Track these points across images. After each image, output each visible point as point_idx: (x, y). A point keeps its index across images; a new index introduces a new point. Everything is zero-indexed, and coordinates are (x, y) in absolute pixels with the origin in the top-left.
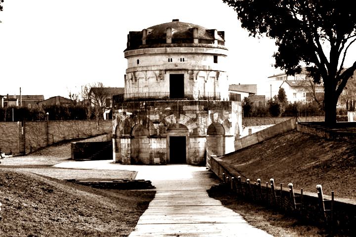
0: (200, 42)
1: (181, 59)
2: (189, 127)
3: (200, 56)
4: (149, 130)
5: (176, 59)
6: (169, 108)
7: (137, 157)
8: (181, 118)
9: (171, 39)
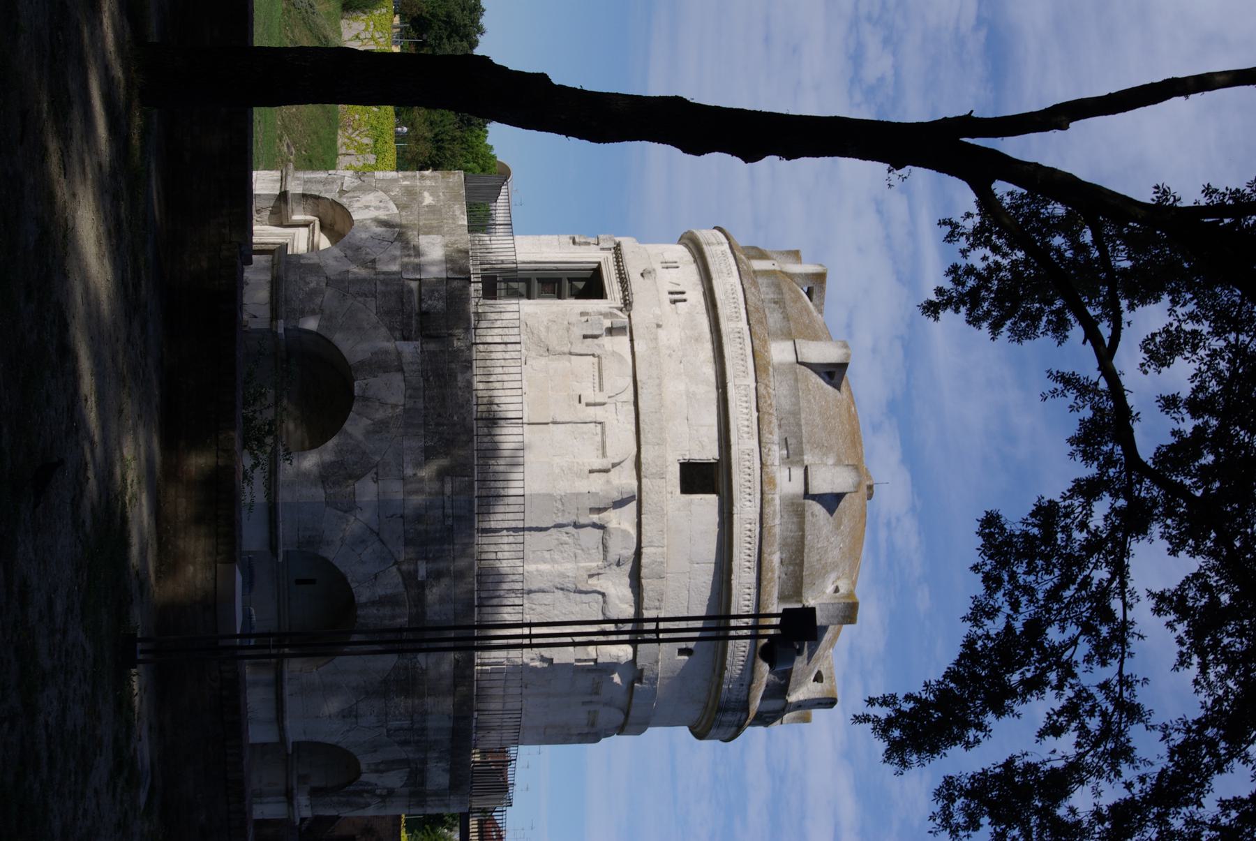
0: (782, 369)
1: (683, 293)
3: (709, 372)
6: (428, 199)
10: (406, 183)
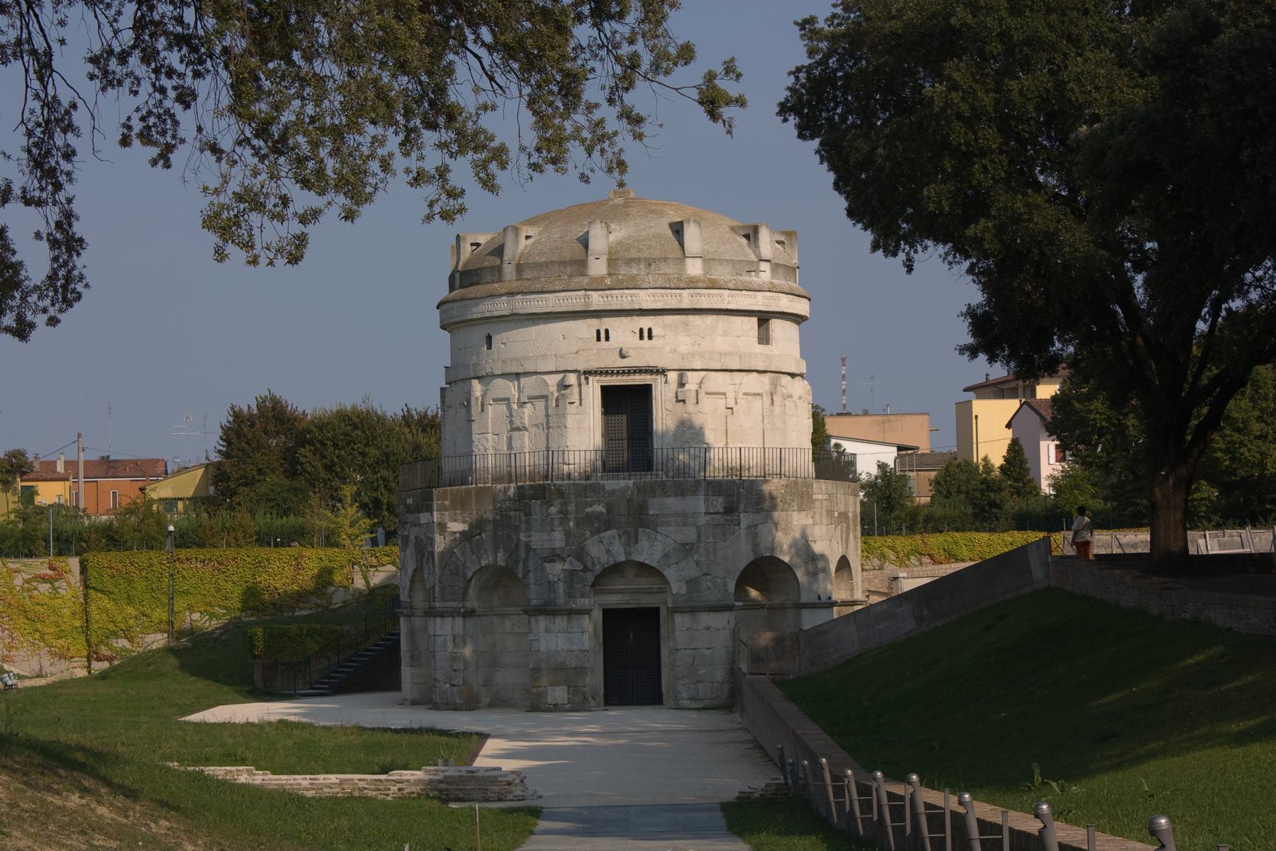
0: (707, 269)
1: (641, 331)
2: (670, 574)
3: (710, 319)
4: (527, 586)
5: (624, 332)
6: (600, 508)
7: (487, 683)
8: (644, 542)
9: (604, 259)
10: (571, 524)
